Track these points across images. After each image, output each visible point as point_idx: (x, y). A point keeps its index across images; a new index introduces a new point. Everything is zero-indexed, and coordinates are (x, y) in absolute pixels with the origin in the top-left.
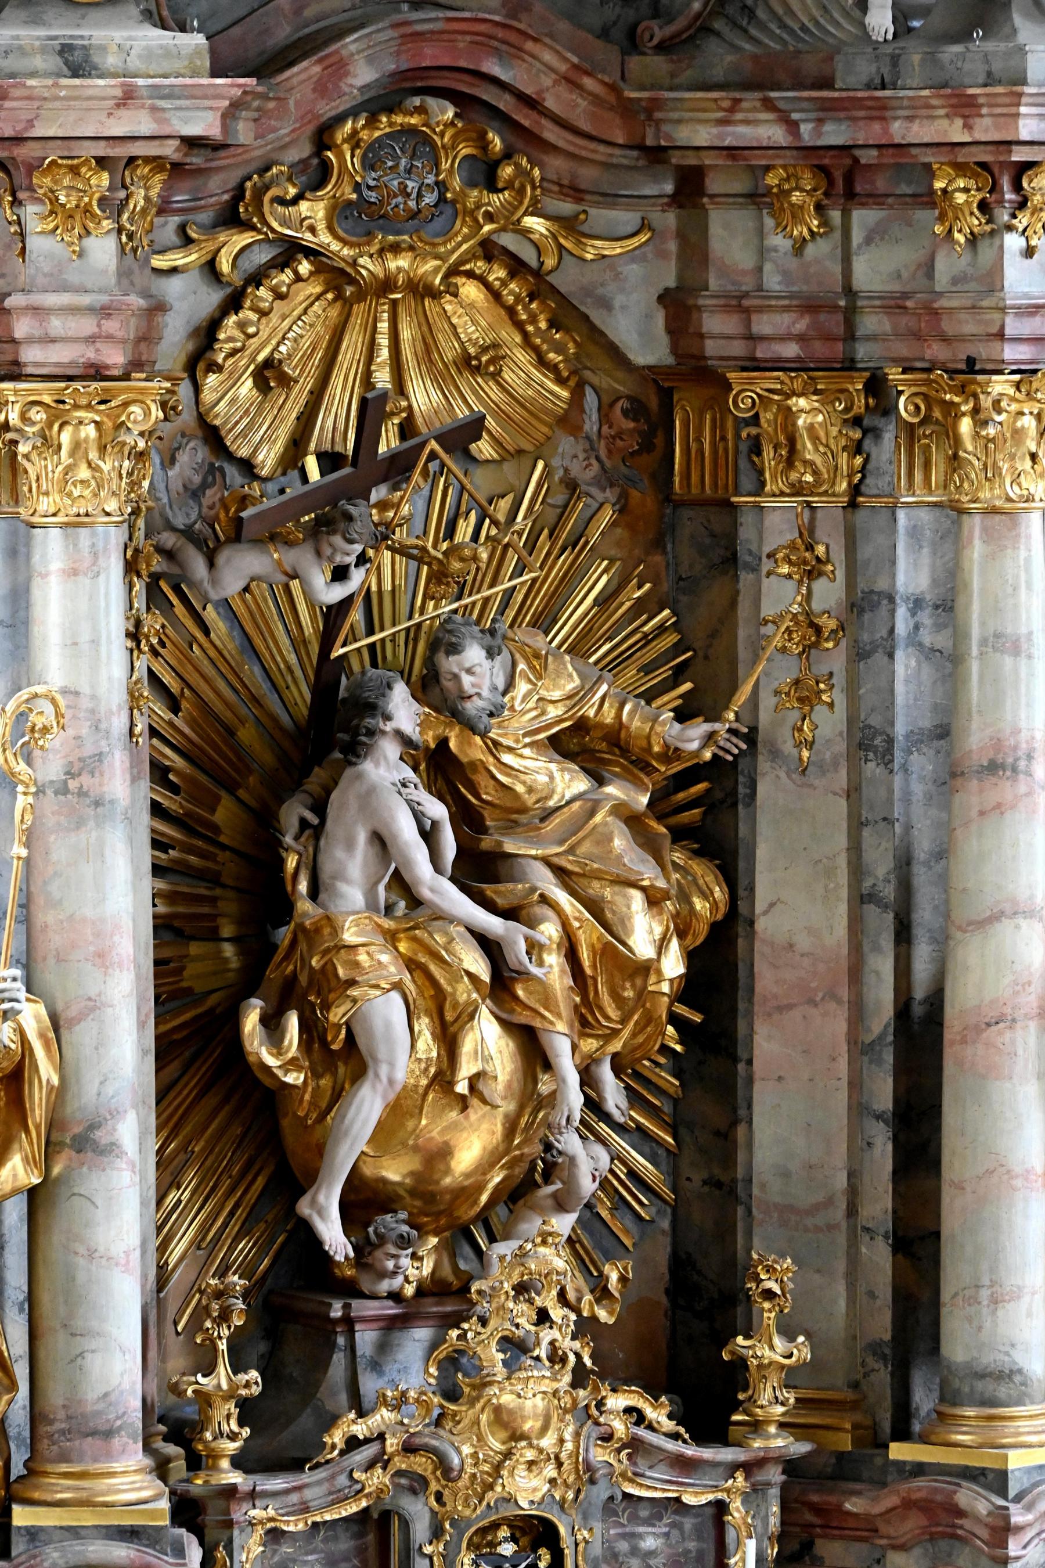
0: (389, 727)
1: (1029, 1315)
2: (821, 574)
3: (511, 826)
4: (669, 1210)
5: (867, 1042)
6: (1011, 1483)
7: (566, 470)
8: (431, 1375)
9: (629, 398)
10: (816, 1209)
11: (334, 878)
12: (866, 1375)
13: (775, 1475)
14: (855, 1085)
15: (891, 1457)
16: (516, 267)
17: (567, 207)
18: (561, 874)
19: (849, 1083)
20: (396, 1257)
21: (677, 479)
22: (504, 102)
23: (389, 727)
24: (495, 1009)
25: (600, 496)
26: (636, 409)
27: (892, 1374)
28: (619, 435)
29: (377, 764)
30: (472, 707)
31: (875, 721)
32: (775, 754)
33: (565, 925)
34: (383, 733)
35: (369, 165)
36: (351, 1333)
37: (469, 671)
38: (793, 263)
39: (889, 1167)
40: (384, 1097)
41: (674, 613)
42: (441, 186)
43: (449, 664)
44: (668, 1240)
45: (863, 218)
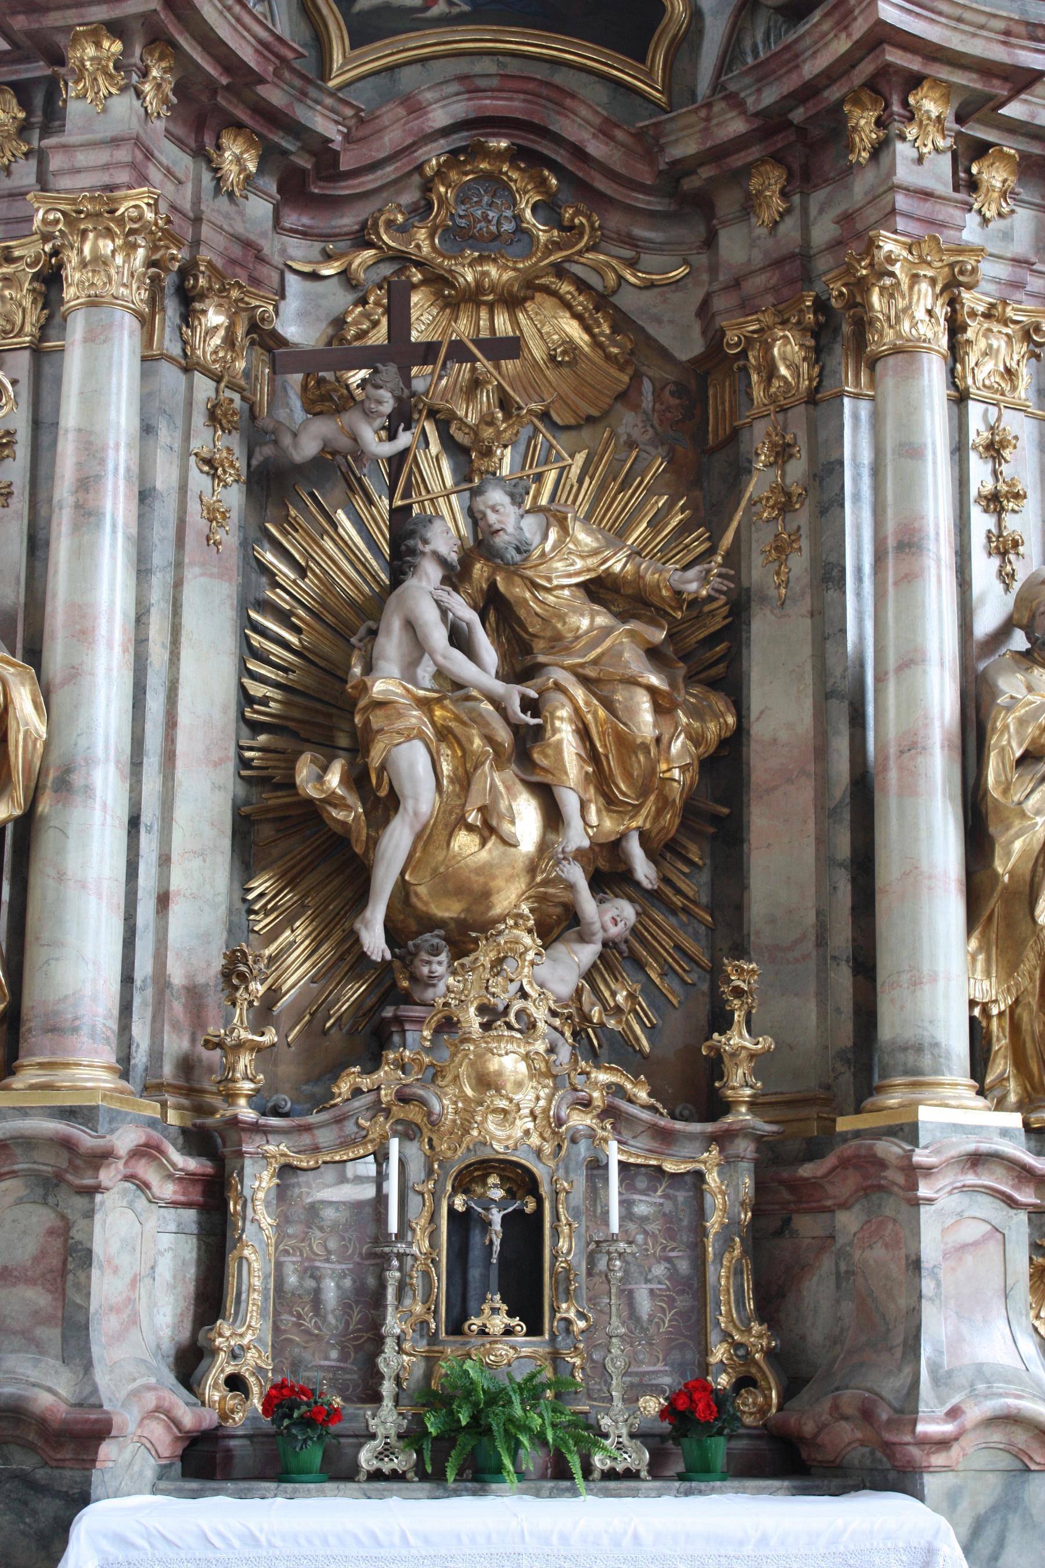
0: (427, 549)
1: (946, 996)
2: (791, 456)
3: (550, 650)
4: (708, 976)
5: (832, 806)
6: (921, 1133)
7: (629, 435)
8: (425, 1039)
9: (674, 383)
10: (796, 942)
11: (378, 659)
12: (836, 1078)
13: (745, 1148)
14: (823, 841)
15: (838, 1129)
16: (582, 286)
17: (629, 253)
18: (585, 681)
19: (817, 839)
20: (429, 963)
21: (711, 436)
22: (560, 156)
23: (427, 549)
24: (519, 773)
25: (653, 452)
26: (680, 390)
27: (855, 1075)
28: (668, 409)
29: (420, 580)
30: (500, 540)
31: (833, 558)
32: (764, 599)
33: (577, 709)
34: (423, 553)
35: (461, 200)
36: (403, 1032)
37: (494, 510)
38: (770, 243)
39: (849, 904)
40: (412, 827)
41: (708, 530)
42: (518, 218)
43: (480, 503)
44: (707, 999)
45: (818, 197)
